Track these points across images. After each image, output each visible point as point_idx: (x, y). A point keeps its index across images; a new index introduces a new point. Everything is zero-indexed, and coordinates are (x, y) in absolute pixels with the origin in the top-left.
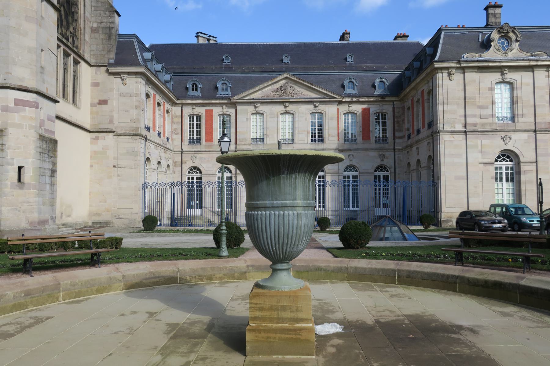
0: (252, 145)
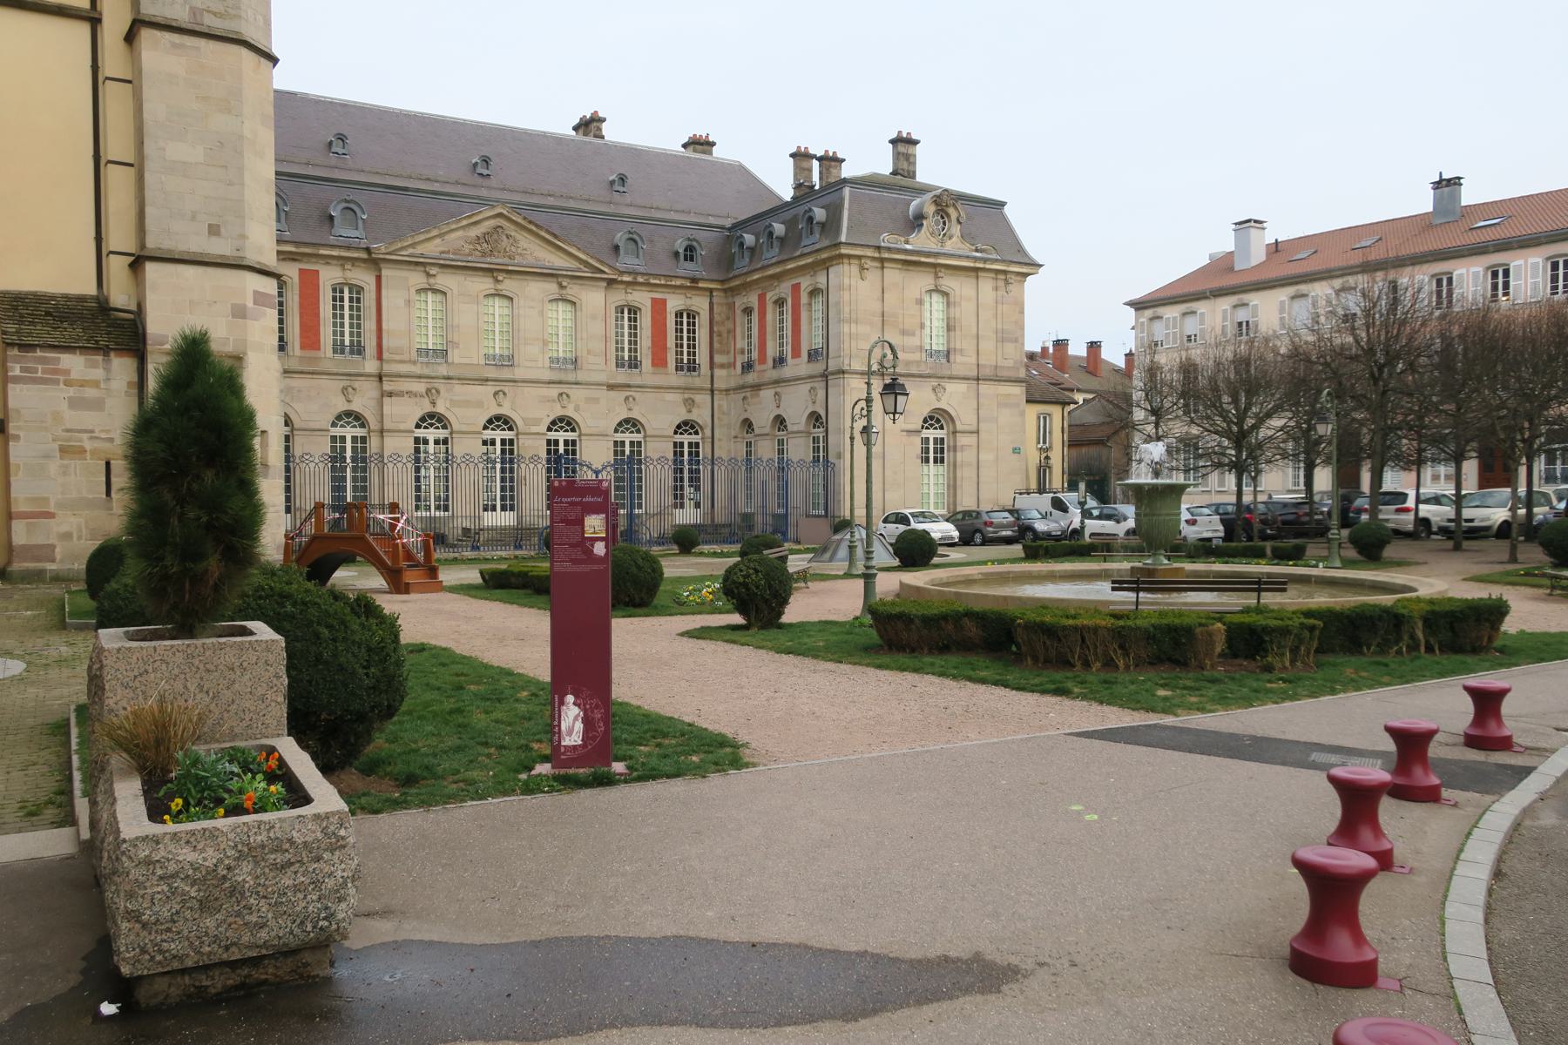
0: (419, 365)
